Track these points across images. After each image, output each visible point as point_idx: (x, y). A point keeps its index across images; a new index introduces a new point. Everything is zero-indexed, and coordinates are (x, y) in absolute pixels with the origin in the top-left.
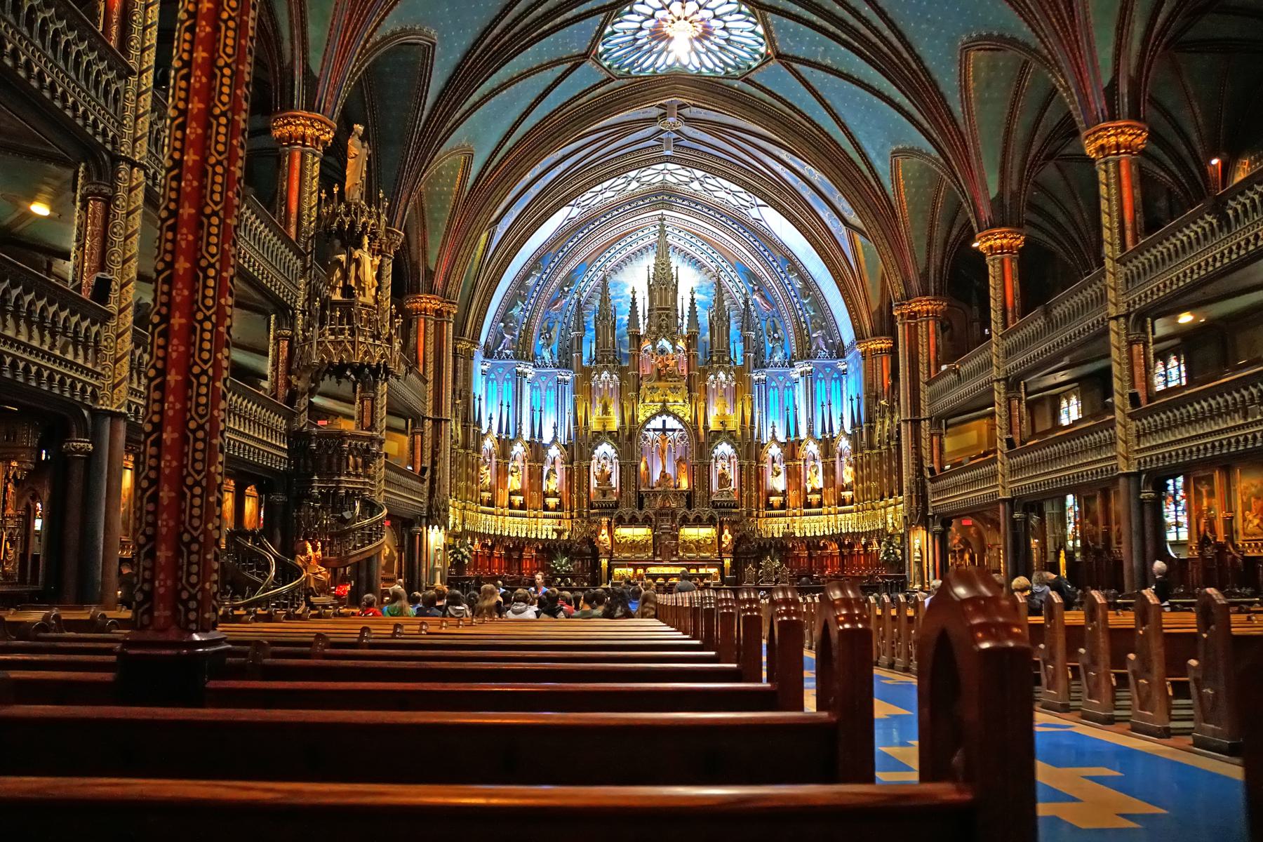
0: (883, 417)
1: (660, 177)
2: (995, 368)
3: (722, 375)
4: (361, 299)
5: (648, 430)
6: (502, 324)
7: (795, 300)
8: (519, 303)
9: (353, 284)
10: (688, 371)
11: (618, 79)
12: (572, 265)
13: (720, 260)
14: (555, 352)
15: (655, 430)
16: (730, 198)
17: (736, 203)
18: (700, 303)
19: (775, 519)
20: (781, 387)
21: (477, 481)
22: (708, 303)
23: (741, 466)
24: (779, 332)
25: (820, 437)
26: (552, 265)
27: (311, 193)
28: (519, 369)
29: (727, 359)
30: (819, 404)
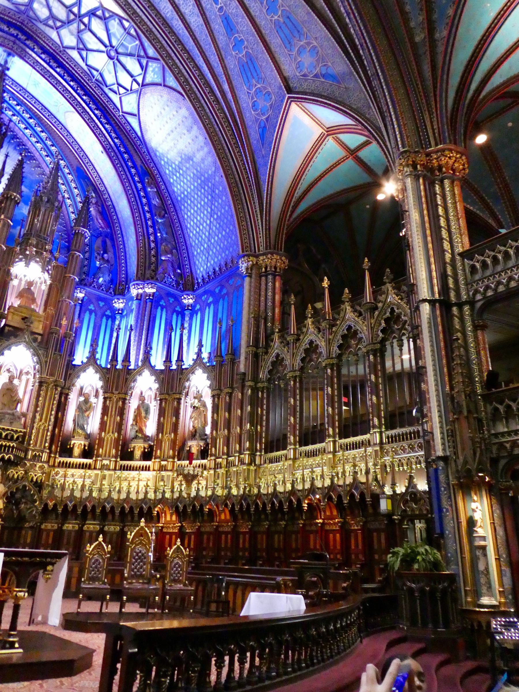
19: (70, 471)
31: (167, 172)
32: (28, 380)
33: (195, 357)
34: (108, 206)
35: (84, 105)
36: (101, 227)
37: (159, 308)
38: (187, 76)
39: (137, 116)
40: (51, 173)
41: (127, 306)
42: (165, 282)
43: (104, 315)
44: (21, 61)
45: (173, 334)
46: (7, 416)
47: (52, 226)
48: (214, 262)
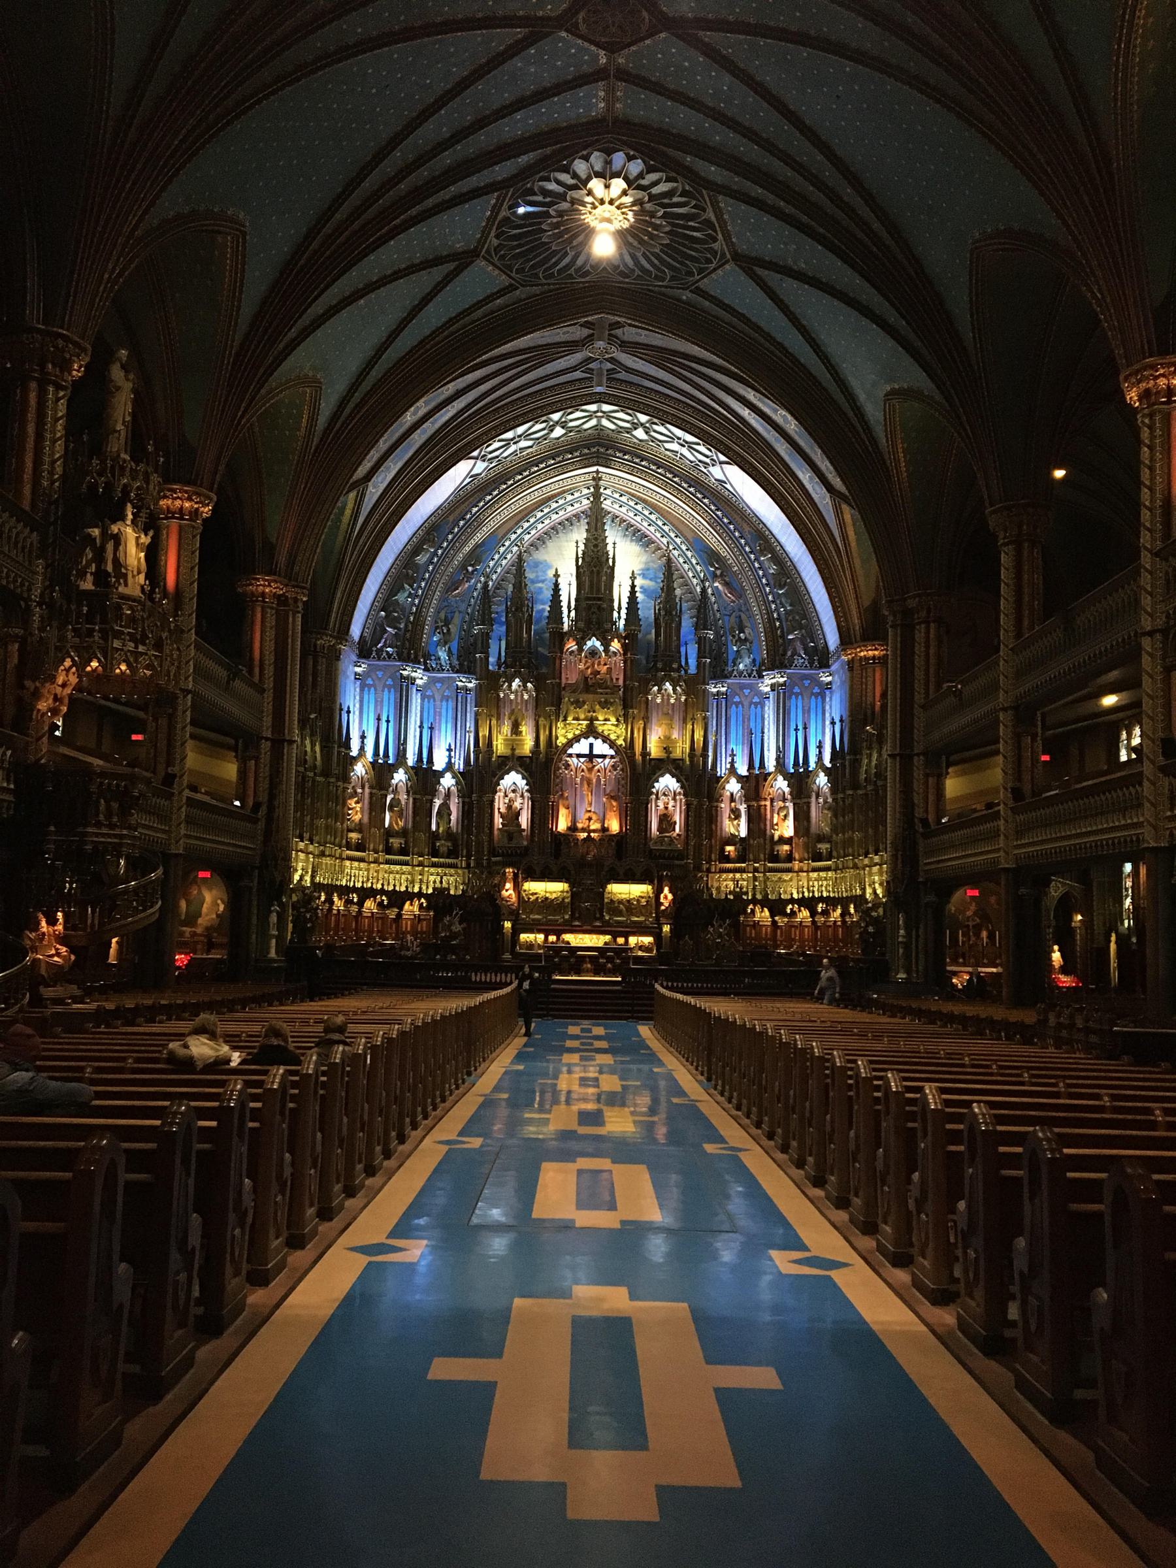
0: (870, 748)
1: (593, 422)
2: (1002, 692)
3: (668, 686)
4: (121, 589)
5: (570, 756)
7: (768, 589)
8: (406, 586)
9: (110, 568)
10: (624, 681)
11: (523, 286)
12: (478, 537)
13: (672, 535)
14: (455, 651)
15: (579, 756)
16: (685, 451)
17: (692, 458)
18: (644, 590)
20: (746, 703)
21: (341, 816)
22: (653, 591)
23: (688, 805)
24: (747, 631)
25: (792, 771)
27: (54, 441)
28: (405, 673)
29: (675, 666)
30: (793, 727)
36: (734, 602)
43: (751, 703)
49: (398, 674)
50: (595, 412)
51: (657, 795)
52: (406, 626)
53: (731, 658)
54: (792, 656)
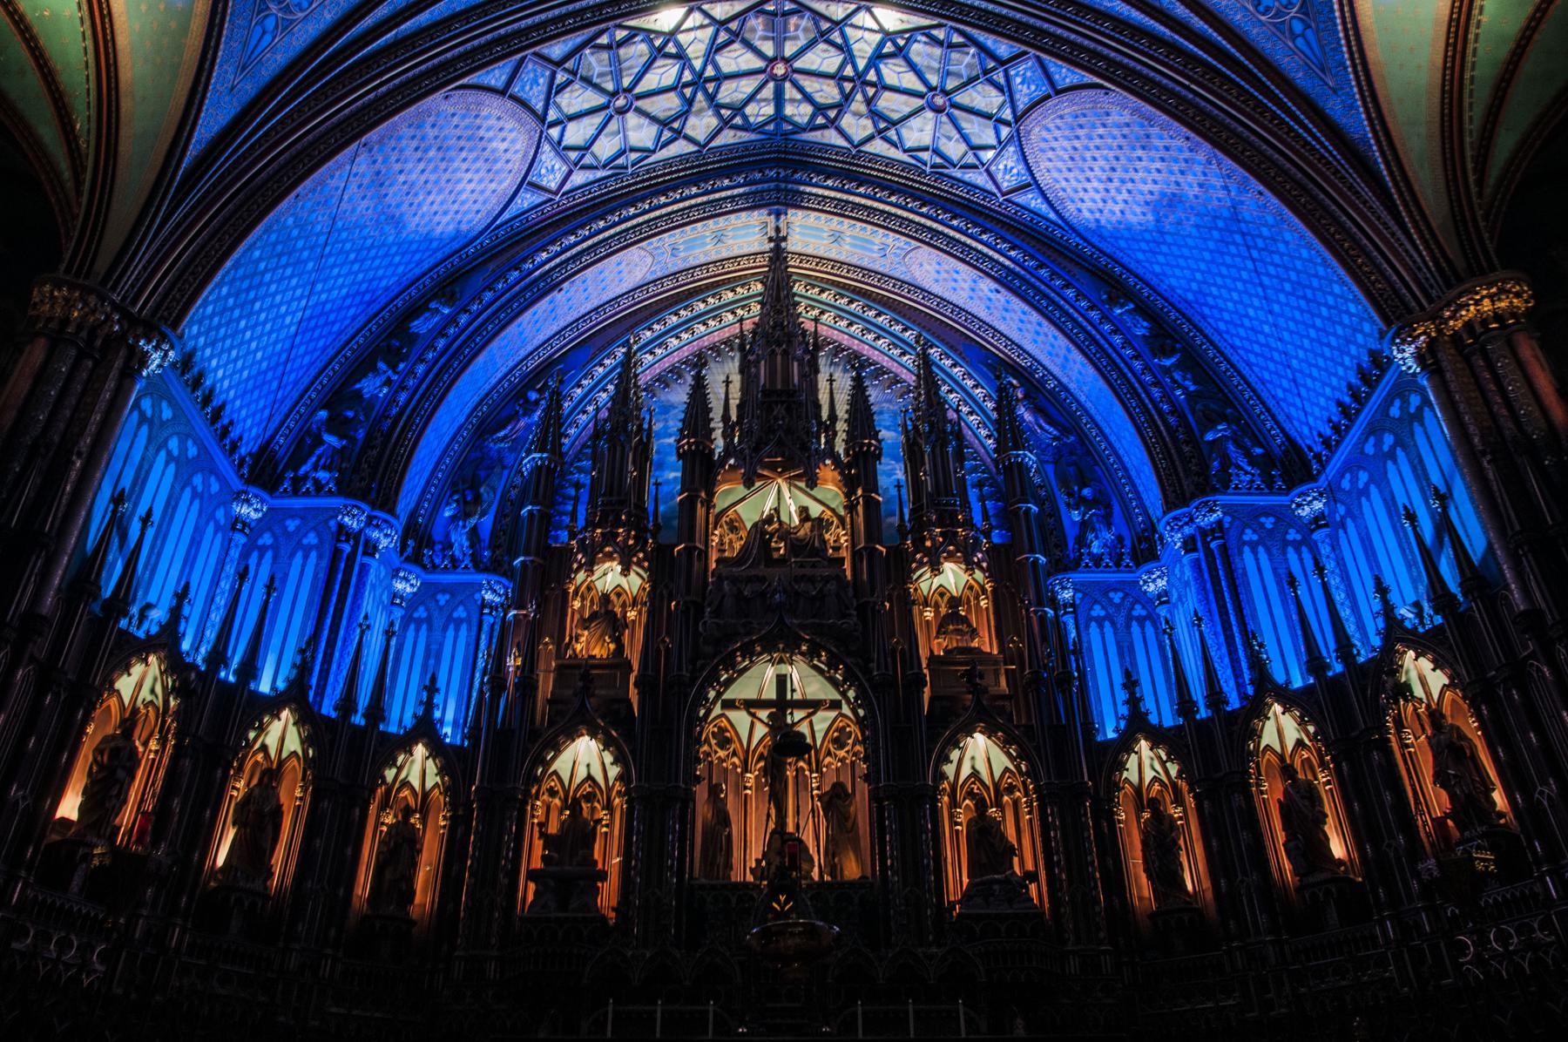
5: (730, 705)
6: (323, 414)
7: (1137, 365)
8: (382, 365)
14: (485, 533)
15: (750, 705)
26: (488, 296)
28: (350, 522)
31: (1140, 256)
32: (1016, 803)
33: (1381, 623)
34: (1051, 392)
35: (929, 223)
36: (1055, 438)
37: (1247, 549)
38: (1092, 45)
39: (1033, 184)
40: (918, 376)
41: (1173, 580)
42: (1236, 487)
43: (1129, 619)
44: (800, 213)
45: (1302, 591)
46: (996, 887)
47: (956, 472)
48: (1333, 389)
49: (332, 523)
50: (771, 61)
51: (953, 795)
52: (369, 437)
53: (1071, 534)
54: (1224, 468)
